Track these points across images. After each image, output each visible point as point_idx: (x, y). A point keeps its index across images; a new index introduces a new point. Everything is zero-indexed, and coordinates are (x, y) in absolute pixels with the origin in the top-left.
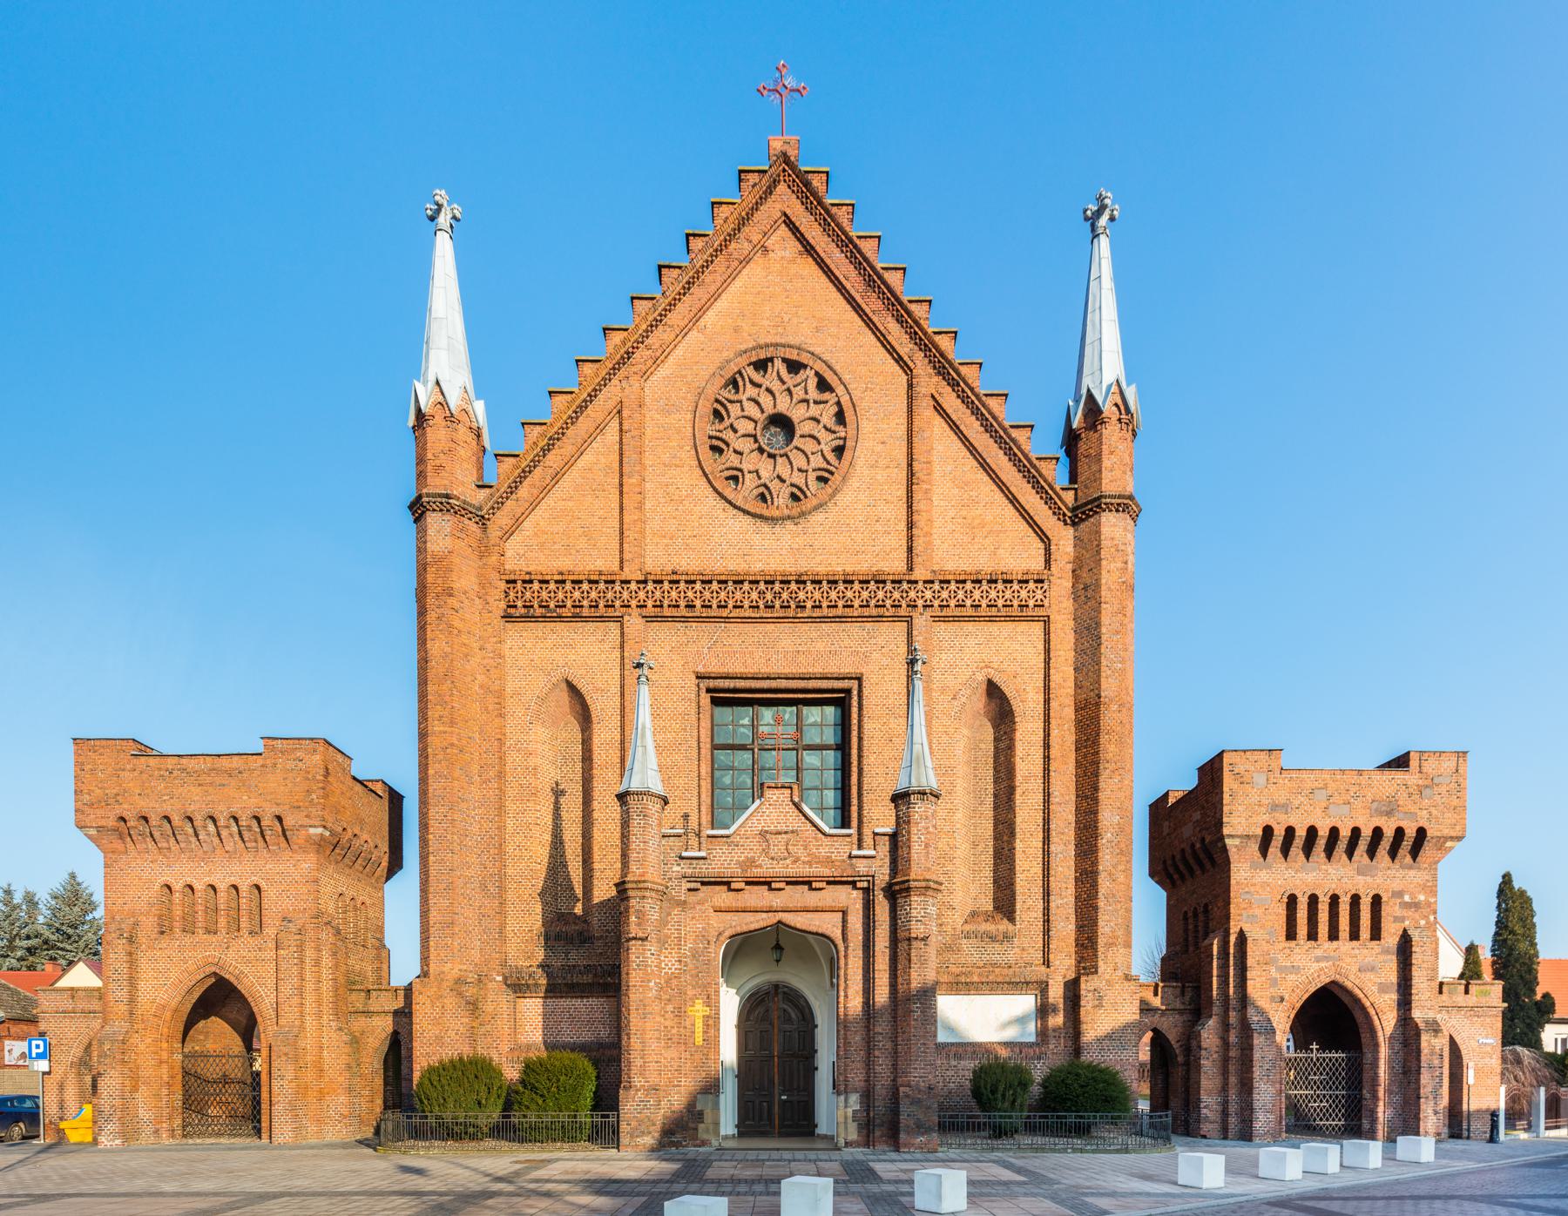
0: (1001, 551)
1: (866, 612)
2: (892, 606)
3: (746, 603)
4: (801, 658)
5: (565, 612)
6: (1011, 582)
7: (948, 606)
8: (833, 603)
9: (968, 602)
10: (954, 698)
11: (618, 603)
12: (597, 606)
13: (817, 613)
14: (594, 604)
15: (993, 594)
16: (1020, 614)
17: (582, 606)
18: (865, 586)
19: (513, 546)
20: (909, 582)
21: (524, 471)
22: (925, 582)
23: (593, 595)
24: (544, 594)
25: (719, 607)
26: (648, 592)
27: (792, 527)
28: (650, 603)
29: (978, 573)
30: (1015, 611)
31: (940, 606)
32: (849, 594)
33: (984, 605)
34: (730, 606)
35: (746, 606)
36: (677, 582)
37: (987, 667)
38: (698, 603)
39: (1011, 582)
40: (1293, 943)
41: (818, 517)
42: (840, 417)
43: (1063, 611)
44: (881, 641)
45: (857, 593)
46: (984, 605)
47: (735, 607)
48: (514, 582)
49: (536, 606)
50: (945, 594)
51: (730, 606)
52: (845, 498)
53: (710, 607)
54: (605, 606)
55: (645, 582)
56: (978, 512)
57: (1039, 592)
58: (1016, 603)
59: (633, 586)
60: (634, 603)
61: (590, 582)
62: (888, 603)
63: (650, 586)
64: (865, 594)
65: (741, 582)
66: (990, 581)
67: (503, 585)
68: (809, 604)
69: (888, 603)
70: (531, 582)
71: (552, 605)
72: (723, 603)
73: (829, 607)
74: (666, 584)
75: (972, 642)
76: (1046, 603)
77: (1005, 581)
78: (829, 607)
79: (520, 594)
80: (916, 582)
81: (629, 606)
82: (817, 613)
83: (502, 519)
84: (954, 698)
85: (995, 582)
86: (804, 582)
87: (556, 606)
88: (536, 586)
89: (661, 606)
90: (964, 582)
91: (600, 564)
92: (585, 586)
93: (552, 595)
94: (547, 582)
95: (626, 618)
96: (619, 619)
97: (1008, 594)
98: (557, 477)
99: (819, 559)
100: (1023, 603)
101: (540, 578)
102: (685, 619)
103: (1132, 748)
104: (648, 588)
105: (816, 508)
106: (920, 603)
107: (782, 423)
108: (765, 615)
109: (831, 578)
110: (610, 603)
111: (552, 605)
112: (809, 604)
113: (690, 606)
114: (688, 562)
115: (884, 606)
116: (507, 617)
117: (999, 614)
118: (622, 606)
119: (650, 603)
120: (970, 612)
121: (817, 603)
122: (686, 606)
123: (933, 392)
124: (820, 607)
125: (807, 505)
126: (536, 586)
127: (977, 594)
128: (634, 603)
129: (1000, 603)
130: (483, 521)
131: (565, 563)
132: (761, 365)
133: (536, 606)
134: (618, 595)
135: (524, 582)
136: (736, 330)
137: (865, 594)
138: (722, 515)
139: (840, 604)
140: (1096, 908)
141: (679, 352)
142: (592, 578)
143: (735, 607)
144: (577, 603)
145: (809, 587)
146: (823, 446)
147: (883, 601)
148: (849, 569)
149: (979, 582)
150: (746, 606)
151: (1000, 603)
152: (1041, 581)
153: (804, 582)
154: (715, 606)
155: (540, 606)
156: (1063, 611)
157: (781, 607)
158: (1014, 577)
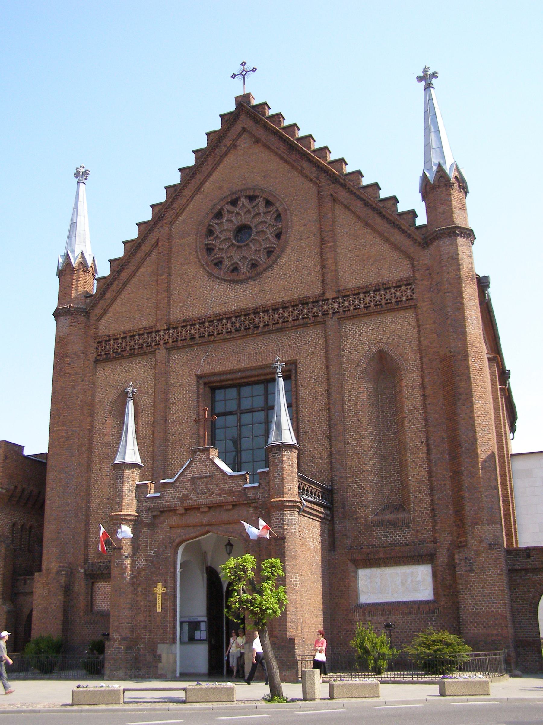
0: (383, 271)
1: (297, 323)
2: (313, 317)
4: (259, 356)
6: (390, 288)
7: (349, 310)
9: (362, 306)
10: (358, 366)
12: (142, 348)
14: (141, 346)
17: (135, 349)
19: (102, 324)
21: (108, 285)
22: (333, 299)
25: (209, 335)
26: (169, 335)
27: (252, 283)
29: (367, 286)
30: (394, 306)
31: (344, 311)
34: (215, 334)
36: (186, 326)
37: (379, 342)
38: (197, 336)
39: (390, 288)
41: (268, 273)
42: (278, 217)
43: (426, 300)
44: (308, 338)
47: (218, 334)
50: (346, 304)
51: (215, 334)
52: (283, 260)
53: (204, 336)
57: (409, 291)
58: (394, 300)
59: (162, 333)
60: (162, 342)
61: (140, 335)
62: (310, 315)
63: (171, 331)
66: (375, 291)
67: (96, 345)
69: (310, 315)
70: (109, 340)
72: (211, 333)
73: (274, 324)
74: (180, 329)
75: (367, 329)
76: (414, 297)
78: (274, 324)
80: (328, 300)
81: (159, 344)
82: (267, 329)
83: (98, 311)
84: (358, 366)
85: (379, 290)
86: (259, 313)
87: (122, 351)
90: (358, 294)
91: (146, 323)
92: (137, 338)
96: (154, 353)
97: (388, 296)
98: (125, 285)
99: (268, 297)
100: (399, 299)
101: (114, 337)
102: (190, 346)
105: (265, 270)
106: (331, 311)
108: (235, 336)
109: (274, 307)
111: (119, 351)
112: (261, 325)
113: (193, 338)
114: (192, 313)
115: (308, 318)
116: (97, 361)
117: (382, 309)
118: (155, 345)
120: (364, 311)
123: (332, 192)
129: (383, 302)
130: (87, 314)
131: (127, 327)
134: (154, 339)
135: (106, 341)
136: (221, 188)
138: (213, 284)
139: (280, 321)
141: (190, 206)
142: (140, 332)
143: (218, 334)
144: (132, 347)
145: (261, 315)
146: (269, 235)
147: (307, 314)
148: (286, 299)
149: (369, 292)
151: (383, 302)
152: (410, 284)
155: (114, 353)
156: (426, 300)
157: (245, 329)
158: (391, 285)
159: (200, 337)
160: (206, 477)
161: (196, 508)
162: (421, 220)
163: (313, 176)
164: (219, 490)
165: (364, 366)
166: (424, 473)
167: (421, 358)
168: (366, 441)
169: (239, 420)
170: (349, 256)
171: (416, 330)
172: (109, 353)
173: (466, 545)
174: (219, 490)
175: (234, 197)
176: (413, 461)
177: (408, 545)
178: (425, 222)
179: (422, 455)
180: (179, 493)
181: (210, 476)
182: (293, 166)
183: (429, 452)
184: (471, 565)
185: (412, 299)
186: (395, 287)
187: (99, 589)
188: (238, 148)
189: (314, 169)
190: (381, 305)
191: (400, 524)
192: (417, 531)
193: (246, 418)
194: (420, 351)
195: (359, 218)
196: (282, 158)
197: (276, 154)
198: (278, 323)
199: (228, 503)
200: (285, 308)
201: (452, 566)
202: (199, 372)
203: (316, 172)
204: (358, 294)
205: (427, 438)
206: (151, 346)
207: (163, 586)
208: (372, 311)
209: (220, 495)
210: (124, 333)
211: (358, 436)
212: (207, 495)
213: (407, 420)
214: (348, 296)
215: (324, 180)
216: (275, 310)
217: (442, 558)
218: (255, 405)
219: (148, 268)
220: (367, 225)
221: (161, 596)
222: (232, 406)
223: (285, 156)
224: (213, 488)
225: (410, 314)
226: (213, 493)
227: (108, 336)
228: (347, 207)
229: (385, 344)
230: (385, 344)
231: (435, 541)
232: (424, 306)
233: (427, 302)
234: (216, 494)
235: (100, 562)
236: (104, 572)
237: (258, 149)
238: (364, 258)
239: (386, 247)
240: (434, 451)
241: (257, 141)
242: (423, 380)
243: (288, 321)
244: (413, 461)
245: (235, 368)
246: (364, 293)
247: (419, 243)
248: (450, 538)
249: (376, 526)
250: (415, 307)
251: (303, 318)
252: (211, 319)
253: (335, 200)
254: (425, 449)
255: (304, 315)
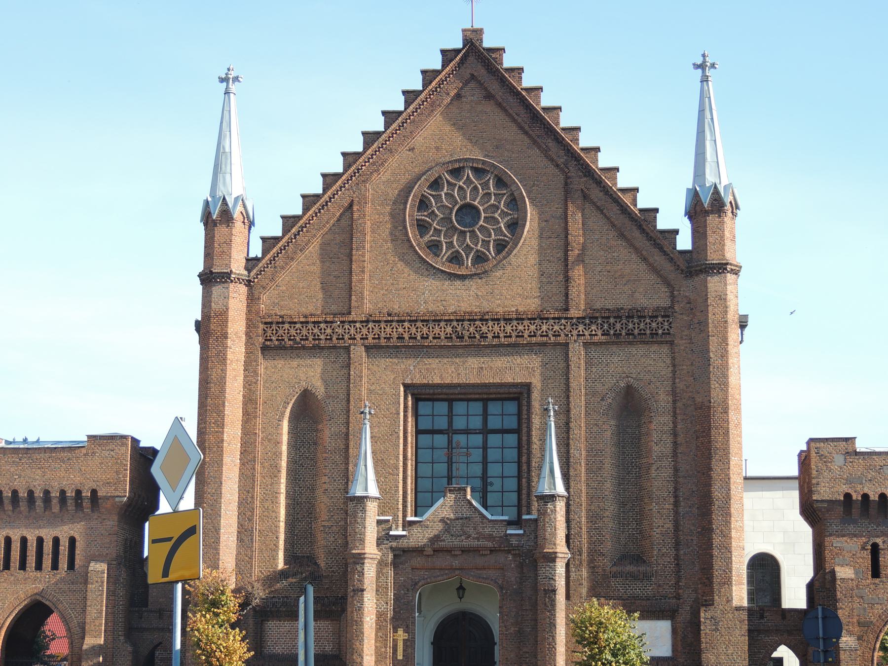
1: (534, 339)
2: (553, 336)
3: (443, 336)
5: (308, 344)
6: (645, 317)
8: (508, 334)
9: (612, 332)
10: (602, 400)
11: (346, 337)
12: (331, 339)
13: (495, 342)
14: (328, 337)
15: (631, 326)
16: (653, 339)
17: (320, 339)
18: (532, 322)
20: (566, 318)
22: (578, 318)
23: (329, 331)
24: (293, 332)
25: (422, 338)
26: (369, 329)
28: (370, 336)
29: (619, 310)
32: (521, 328)
33: (624, 334)
34: (431, 338)
35: (443, 337)
36: (392, 321)
37: (627, 377)
38: (406, 336)
40: (877, 581)
43: (684, 338)
45: (527, 327)
46: (624, 334)
48: (271, 323)
49: (286, 340)
53: (415, 338)
54: (337, 339)
55: (367, 321)
56: (619, 267)
57: (666, 324)
58: (648, 332)
60: (358, 336)
61: (326, 322)
62: (550, 333)
63: (371, 325)
64: (533, 328)
65: (440, 321)
66: (628, 317)
68: (490, 336)
70: (283, 323)
71: (298, 339)
72: (425, 336)
73: (505, 337)
75: (616, 359)
76: (672, 331)
77: (639, 317)
78: (505, 337)
79: (274, 332)
80: (572, 318)
84: (602, 400)
85: (633, 317)
87: (301, 340)
88: (287, 326)
89: (379, 338)
93: (298, 331)
94: (295, 323)
95: (352, 347)
96: (347, 349)
97: (642, 326)
100: (654, 332)
103: (740, 437)
104: (370, 325)
107: (468, 212)
110: (341, 337)
112: (490, 336)
113: (400, 338)
114: (400, 305)
117: (635, 340)
118: (349, 339)
119: (370, 336)
121: (496, 334)
122: (397, 338)
124: (498, 337)
125: (488, 266)
126: (287, 326)
127: (618, 326)
128: (358, 336)
129: (636, 332)
132: (456, 172)
133: (286, 340)
134: (347, 331)
135: (278, 323)
137: (533, 328)
139: (514, 334)
140: (712, 556)
142: (328, 319)
143: (434, 338)
147: (546, 332)
148: (521, 309)
149: (621, 317)
150: (443, 337)
151: (636, 332)
152: (668, 316)
153: (487, 320)
154: (419, 338)
155: (289, 340)
156: (684, 338)
159: (410, 338)
160: (461, 519)
161: (448, 551)
162: (684, 242)
163: (561, 161)
164: (477, 533)
165: (610, 401)
166: (669, 525)
167: (674, 402)
168: (608, 485)
169: (450, 442)
170: (599, 269)
171: (670, 369)
172: (283, 340)
173: (713, 604)
174: (477, 533)
175: (457, 166)
176: (659, 512)
177: (649, 599)
178: (688, 247)
179: (669, 506)
180: (430, 533)
181: (466, 518)
182: (535, 142)
183: (676, 504)
184: (716, 624)
185: (669, 334)
186: (650, 317)
187: (270, 629)
188: (464, 99)
189: (562, 153)
190: (633, 334)
191: (641, 576)
192: (660, 586)
193: (461, 439)
194: (674, 392)
195: (614, 225)
196: (521, 128)
197: (514, 121)
198: (510, 337)
199: (486, 548)
200: (520, 320)
201: (695, 625)
202: (408, 381)
203: (565, 158)
204: (609, 318)
205: (676, 489)
206: (343, 339)
207: (405, 631)
208: (623, 340)
209: (478, 539)
210: (306, 317)
211: (599, 478)
212: (463, 537)
213: (654, 467)
214: (597, 318)
215: (573, 171)
216: (508, 320)
217: (684, 614)
218: (471, 426)
219: (336, 235)
220: (622, 236)
221: (402, 642)
222: (442, 423)
223: (526, 127)
224: (471, 531)
225: (665, 349)
226: (469, 536)
227: (281, 317)
228: (600, 209)
229: (634, 379)
230: (634, 379)
231: (678, 597)
232: (681, 344)
233: (685, 339)
234: (474, 538)
235: (274, 597)
236: (281, 609)
237: (489, 107)
238: (616, 276)
239: (643, 266)
240: (682, 504)
241: (489, 96)
242: (675, 426)
243: (523, 336)
244: (659, 512)
245: (454, 382)
246: (615, 317)
247: (682, 271)
248: (694, 596)
249: (615, 576)
250: (671, 343)
251: (542, 336)
252: (426, 318)
253: (585, 197)
254: (672, 500)
255: (543, 332)
